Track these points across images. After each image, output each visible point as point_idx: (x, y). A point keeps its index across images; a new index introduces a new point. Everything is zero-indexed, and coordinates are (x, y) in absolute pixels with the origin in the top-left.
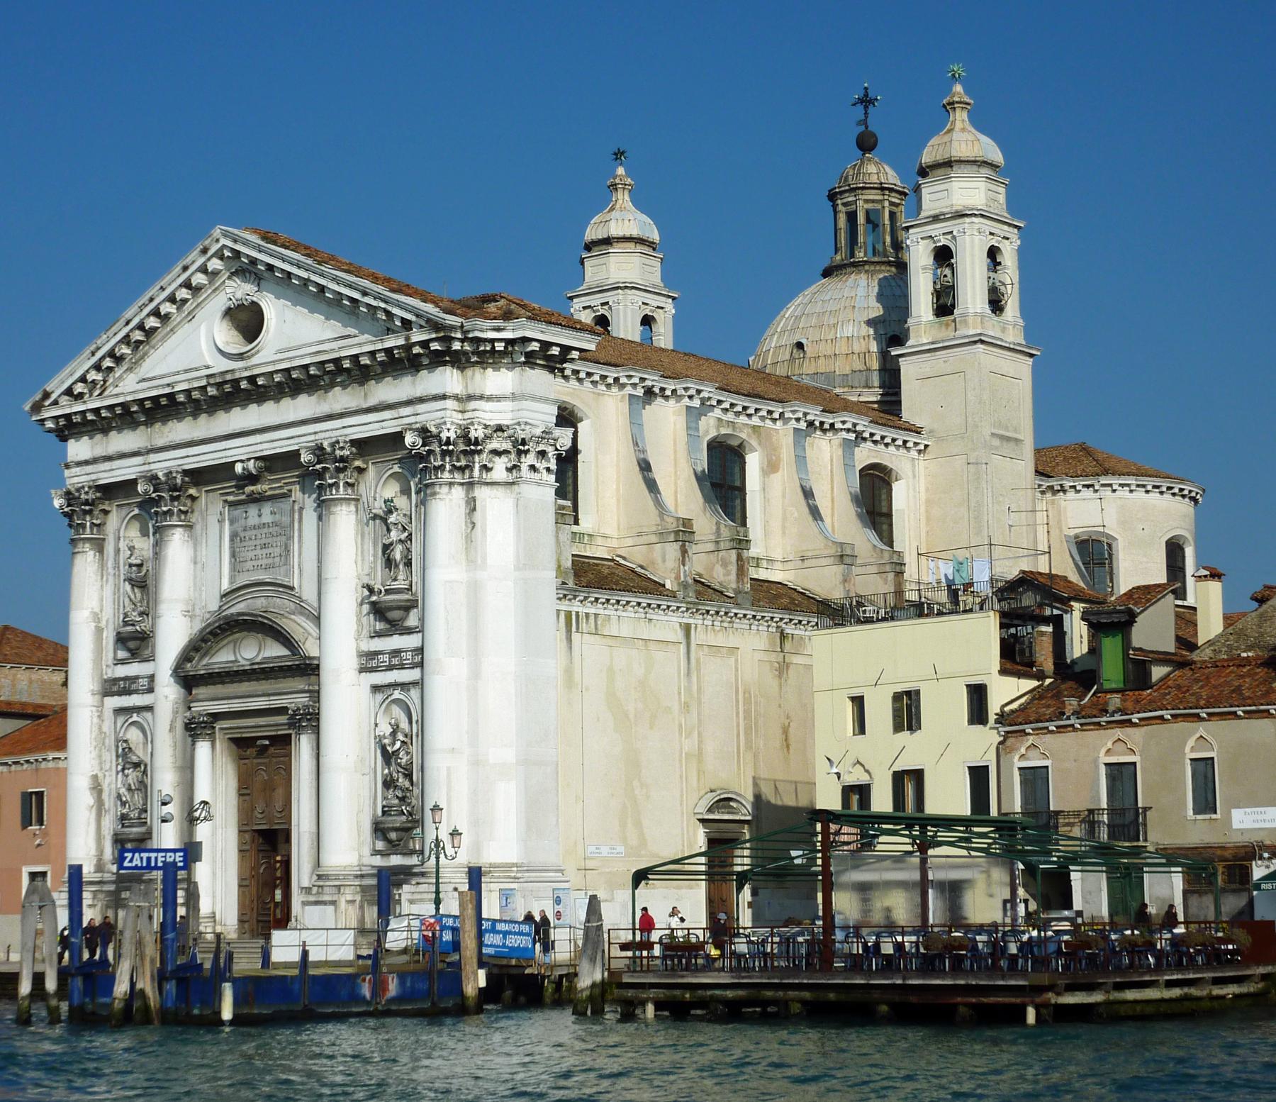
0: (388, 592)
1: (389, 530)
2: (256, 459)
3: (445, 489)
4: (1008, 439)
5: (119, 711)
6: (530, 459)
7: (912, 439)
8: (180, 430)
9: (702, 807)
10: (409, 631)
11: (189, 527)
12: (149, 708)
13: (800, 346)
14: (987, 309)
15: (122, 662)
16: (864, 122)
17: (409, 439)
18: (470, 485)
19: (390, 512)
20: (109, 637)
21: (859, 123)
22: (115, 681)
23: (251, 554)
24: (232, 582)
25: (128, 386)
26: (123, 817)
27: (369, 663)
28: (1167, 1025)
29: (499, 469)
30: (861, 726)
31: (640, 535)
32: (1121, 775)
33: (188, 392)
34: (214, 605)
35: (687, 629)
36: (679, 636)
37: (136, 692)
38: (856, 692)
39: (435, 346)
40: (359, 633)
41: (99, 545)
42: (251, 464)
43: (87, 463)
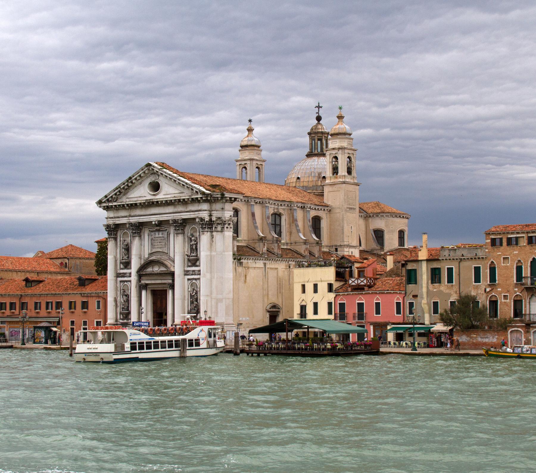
0: (192, 256)
1: (191, 241)
3: (206, 233)
4: (351, 209)
5: (121, 281)
6: (226, 226)
7: (326, 209)
8: (138, 212)
9: (268, 308)
10: (197, 266)
11: (140, 236)
12: (130, 281)
13: (298, 178)
14: (346, 174)
15: (122, 269)
16: (318, 113)
17: (197, 220)
18: (212, 232)
19: (193, 236)
20: (118, 262)
21: (317, 113)
22: (120, 274)
23: (156, 244)
24: (151, 250)
25: (125, 200)
26: (123, 308)
27: (186, 273)
28: (294, 358)
29: (219, 228)
30: (304, 291)
31: (253, 240)
32: (360, 306)
33: (140, 203)
34: (147, 256)
35: (265, 264)
36: (262, 266)
37: (126, 277)
38: (303, 283)
39: (204, 198)
40: (184, 265)
41: (116, 239)
43: (112, 218)
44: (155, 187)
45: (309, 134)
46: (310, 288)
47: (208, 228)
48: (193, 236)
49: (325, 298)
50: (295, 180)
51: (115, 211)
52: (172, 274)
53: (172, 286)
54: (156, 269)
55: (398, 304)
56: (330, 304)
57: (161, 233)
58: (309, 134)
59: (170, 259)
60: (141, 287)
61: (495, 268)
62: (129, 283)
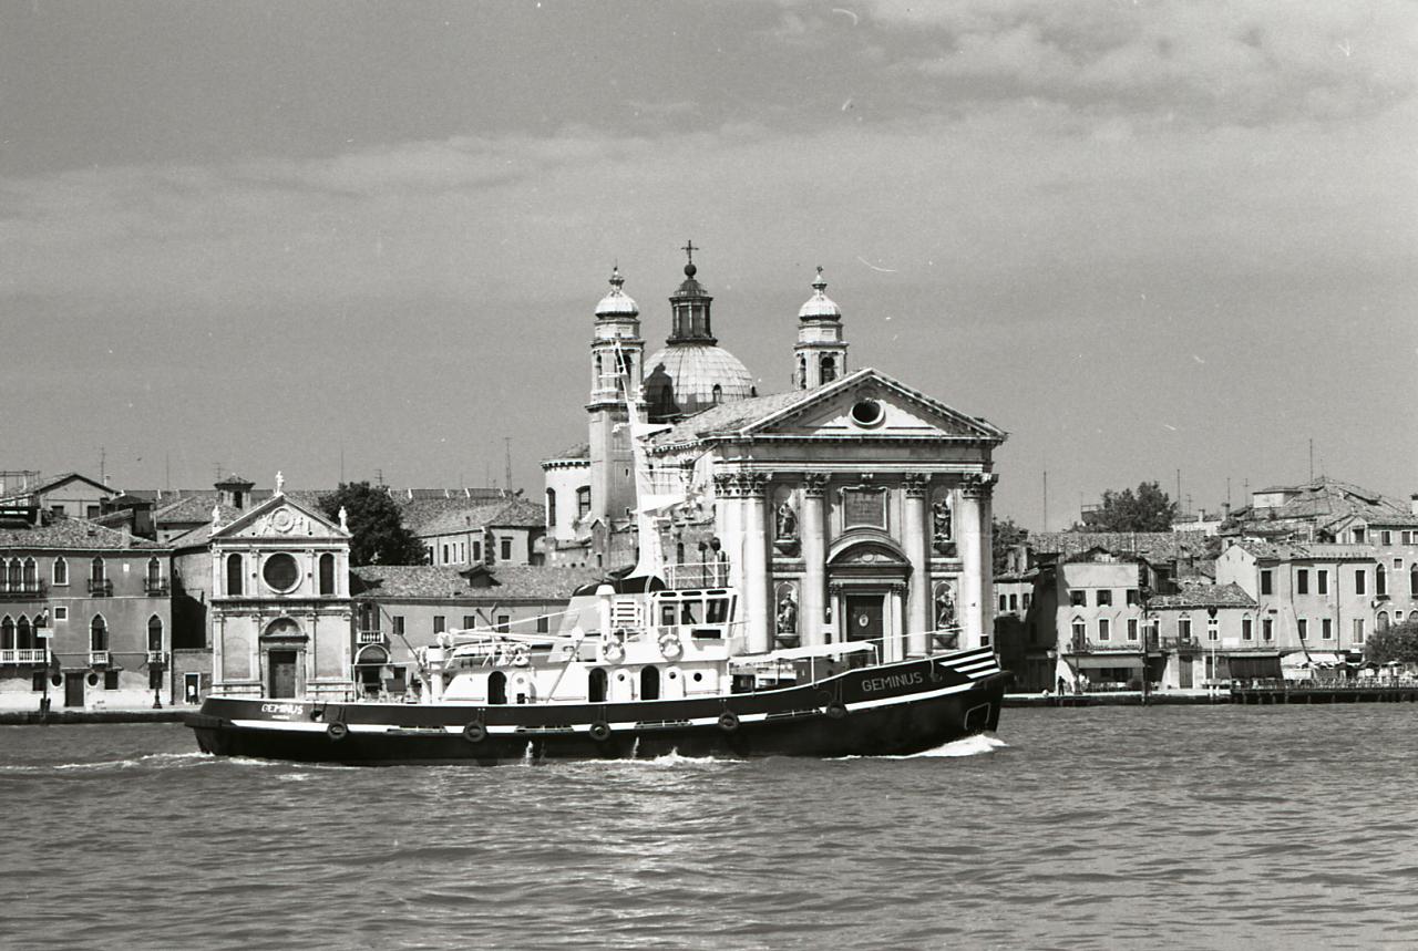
2: (874, 474)
8: (827, 453)
12: (797, 579)
13: (717, 387)
15: (778, 556)
37: (788, 571)
42: (871, 476)
44: (866, 413)
45: (673, 301)
46: (1091, 598)
47: (981, 493)
48: (944, 505)
49: (1122, 611)
50: (710, 390)
51: (771, 449)
52: (907, 571)
53: (904, 593)
54: (868, 558)
55: (1247, 624)
56: (1132, 623)
57: (868, 498)
58: (673, 301)
59: (892, 541)
60: (828, 591)
61: (1384, 573)
62: (795, 583)
